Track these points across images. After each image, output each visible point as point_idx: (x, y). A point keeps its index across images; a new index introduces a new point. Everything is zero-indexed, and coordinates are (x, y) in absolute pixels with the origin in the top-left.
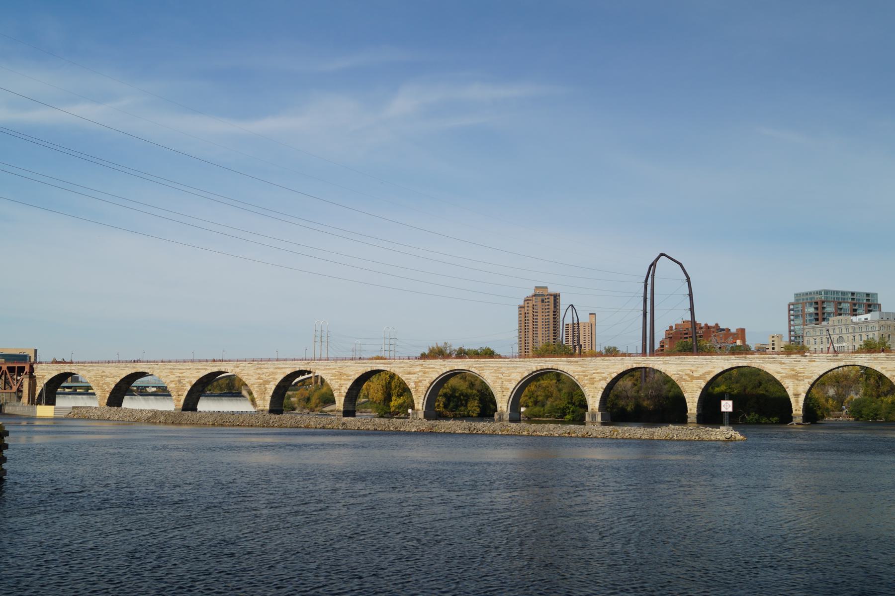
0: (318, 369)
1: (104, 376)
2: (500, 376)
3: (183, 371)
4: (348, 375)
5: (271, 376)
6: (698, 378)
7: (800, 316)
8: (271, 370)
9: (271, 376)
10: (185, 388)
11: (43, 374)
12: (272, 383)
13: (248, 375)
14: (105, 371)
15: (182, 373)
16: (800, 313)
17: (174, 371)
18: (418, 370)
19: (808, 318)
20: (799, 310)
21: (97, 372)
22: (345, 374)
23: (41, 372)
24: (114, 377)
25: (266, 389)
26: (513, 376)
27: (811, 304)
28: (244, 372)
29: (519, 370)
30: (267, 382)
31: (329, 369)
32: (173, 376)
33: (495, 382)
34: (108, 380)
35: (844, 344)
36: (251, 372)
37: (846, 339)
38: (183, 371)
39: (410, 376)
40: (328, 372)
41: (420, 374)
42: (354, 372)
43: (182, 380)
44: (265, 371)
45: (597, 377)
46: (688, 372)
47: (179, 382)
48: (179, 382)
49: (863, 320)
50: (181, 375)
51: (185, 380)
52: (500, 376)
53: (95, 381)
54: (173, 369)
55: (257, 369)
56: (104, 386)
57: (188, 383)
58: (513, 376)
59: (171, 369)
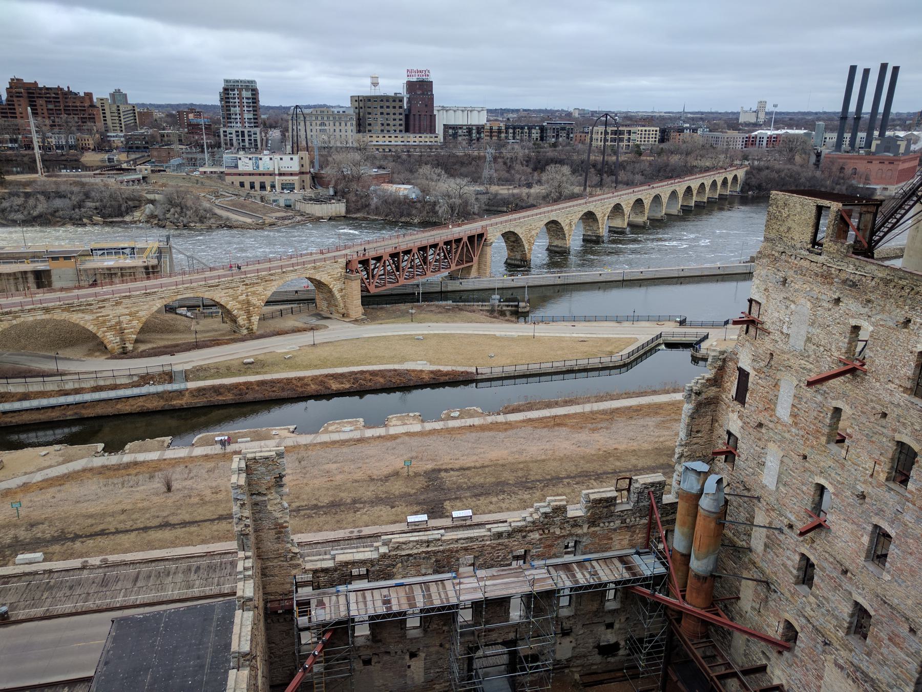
27: (247, 90)
47: (570, 224)
49: (336, 112)
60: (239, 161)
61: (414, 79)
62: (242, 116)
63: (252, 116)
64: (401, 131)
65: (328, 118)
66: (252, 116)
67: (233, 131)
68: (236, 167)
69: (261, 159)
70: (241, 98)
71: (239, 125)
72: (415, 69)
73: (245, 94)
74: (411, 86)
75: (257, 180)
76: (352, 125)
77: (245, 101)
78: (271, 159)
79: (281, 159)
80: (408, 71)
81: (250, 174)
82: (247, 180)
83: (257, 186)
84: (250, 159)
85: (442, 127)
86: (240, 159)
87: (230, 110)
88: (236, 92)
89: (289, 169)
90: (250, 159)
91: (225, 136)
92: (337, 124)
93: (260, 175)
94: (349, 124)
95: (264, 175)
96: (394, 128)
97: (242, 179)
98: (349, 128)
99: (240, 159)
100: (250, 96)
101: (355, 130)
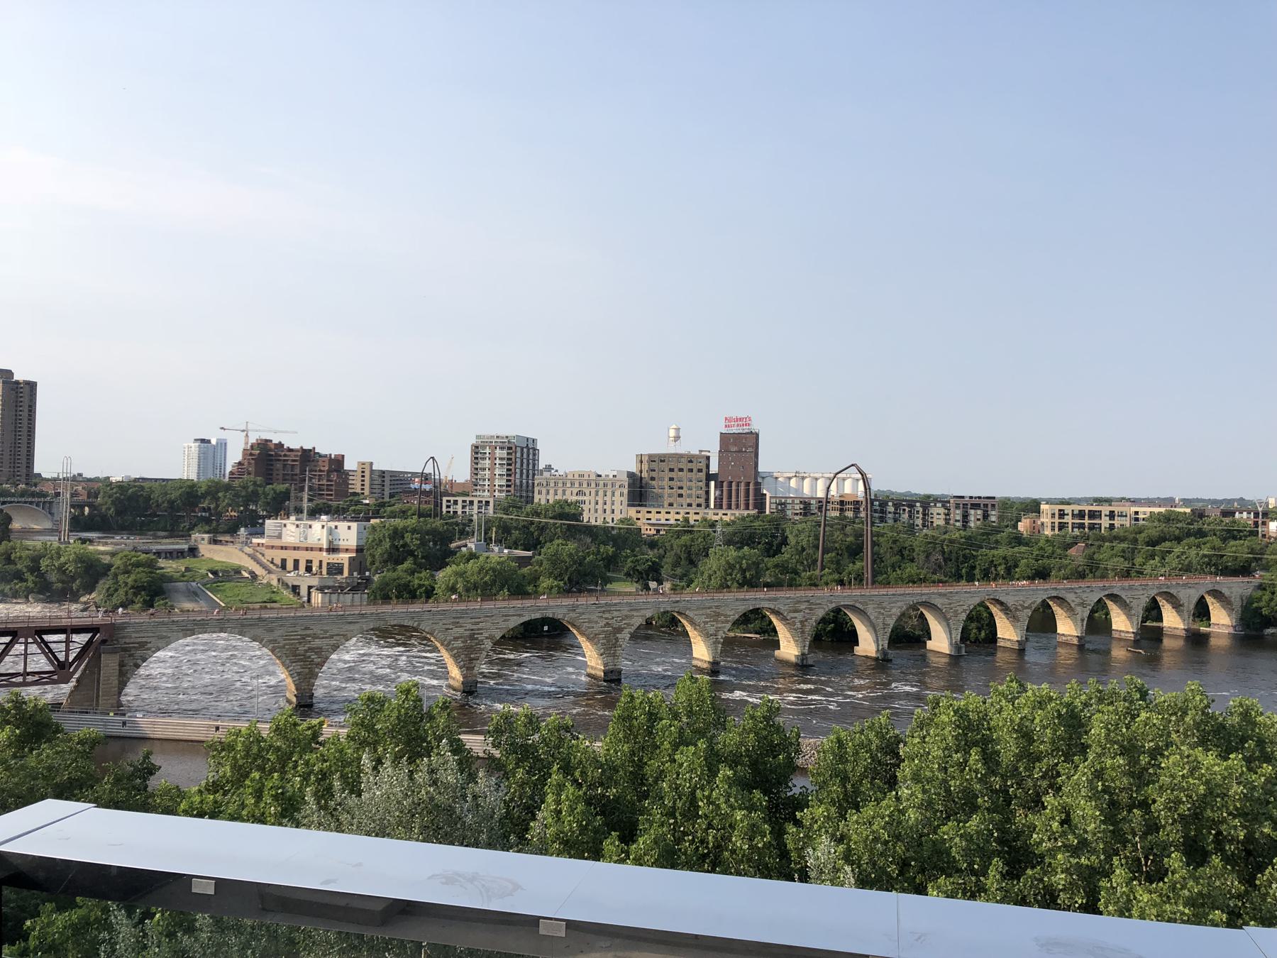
0: (689, 609)
1: (309, 636)
2: (882, 611)
3: (479, 620)
4: (726, 616)
5: (624, 622)
6: (1027, 608)
8: (625, 613)
9: (624, 622)
10: (483, 646)
11: (140, 640)
12: (626, 631)
13: (589, 622)
14: (311, 627)
15: (477, 623)
17: (461, 621)
18: (804, 607)
19: (498, 462)
21: (291, 629)
22: (722, 615)
23: (133, 635)
24: (332, 637)
25: (617, 639)
26: (894, 610)
27: (502, 448)
28: (583, 617)
29: (899, 604)
30: (620, 630)
31: (703, 608)
32: (461, 630)
33: (877, 618)
34: (317, 642)
35: (585, 498)
36: (594, 617)
37: (588, 493)
38: (479, 620)
39: (796, 615)
40: (701, 612)
41: (807, 611)
42: (733, 612)
43: (478, 634)
44: (616, 614)
45: (960, 610)
46: (1022, 603)
48: (472, 637)
50: (474, 627)
51: (482, 634)
52: (882, 611)
53: (287, 647)
54: (461, 618)
55: (604, 612)
56: (308, 654)
57: (487, 638)
58: (894, 610)
59: (454, 618)
60: (284, 529)
61: (735, 430)
63: (504, 483)
64: (699, 505)
65: (589, 485)
66: (504, 483)
67: (476, 500)
68: (279, 537)
69: (310, 527)
71: (486, 493)
74: (727, 441)
75: (303, 556)
76: (622, 495)
77: (498, 462)
80: (726, 419)
81: (295, 548)
82: (290, 556)
83: (290, 565)
88: (488, 451)
91: (448, 507)
92: (601, 493)
93: (307, 549)
94: (617, 493)
95: (312, 549)
96: (688, 501)
97: (284, 554)
98: (617, 498)
100: (505, 456)
101: (625, 502)
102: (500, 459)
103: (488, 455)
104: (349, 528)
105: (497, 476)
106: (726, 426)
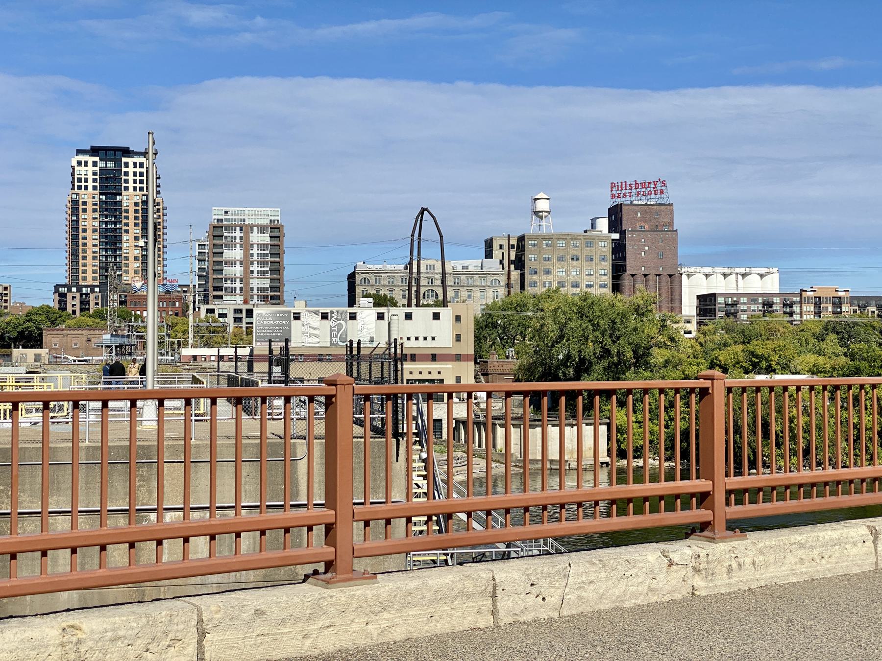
7: (238, 246)
16: (238, 240)
20: (235, 238)
27: (261, 229)
60: (294, 323)
62: (247, 284)
66: (266, 283)
70: (246, 245)
72: (631, 180)
73: (256, 237)
77: (255, 251)
78: (380, 316)
79: (408, 316)
80: (613, 185)
81: (320, 358)
84: (325, 316)
85: (695, 302)
86: (297, 317)
87: (221, 271)
89: (429, 343)
90: (325, 316)
99: (297, 317)
102: (261, 246)
103: (238, 240)
104: (436, 316)
105: (255, 274)
106: (613, 196)
